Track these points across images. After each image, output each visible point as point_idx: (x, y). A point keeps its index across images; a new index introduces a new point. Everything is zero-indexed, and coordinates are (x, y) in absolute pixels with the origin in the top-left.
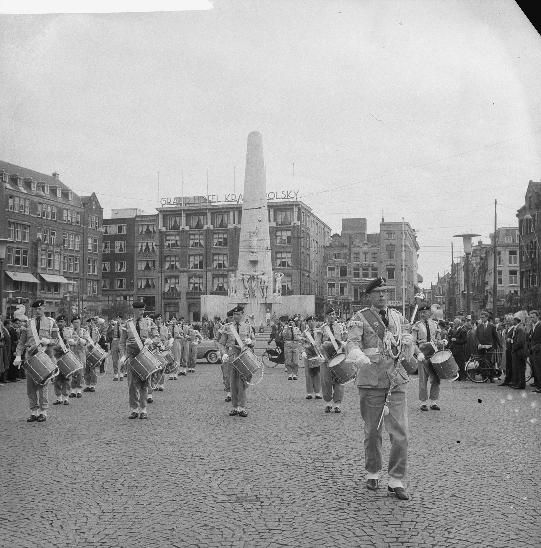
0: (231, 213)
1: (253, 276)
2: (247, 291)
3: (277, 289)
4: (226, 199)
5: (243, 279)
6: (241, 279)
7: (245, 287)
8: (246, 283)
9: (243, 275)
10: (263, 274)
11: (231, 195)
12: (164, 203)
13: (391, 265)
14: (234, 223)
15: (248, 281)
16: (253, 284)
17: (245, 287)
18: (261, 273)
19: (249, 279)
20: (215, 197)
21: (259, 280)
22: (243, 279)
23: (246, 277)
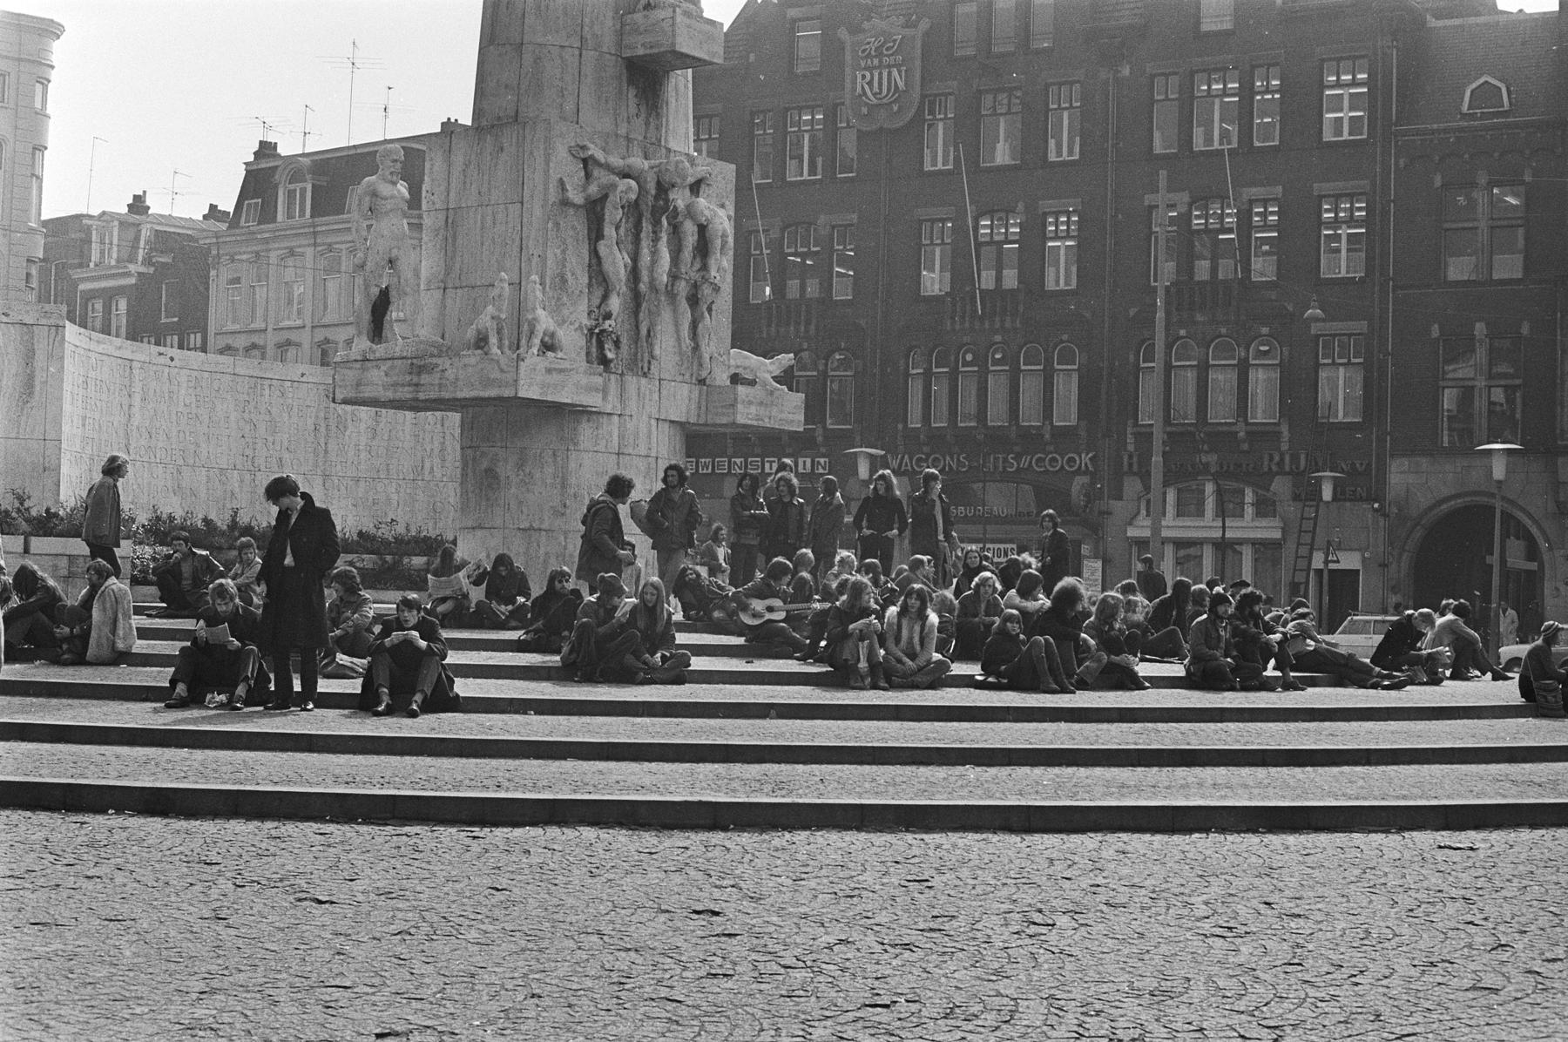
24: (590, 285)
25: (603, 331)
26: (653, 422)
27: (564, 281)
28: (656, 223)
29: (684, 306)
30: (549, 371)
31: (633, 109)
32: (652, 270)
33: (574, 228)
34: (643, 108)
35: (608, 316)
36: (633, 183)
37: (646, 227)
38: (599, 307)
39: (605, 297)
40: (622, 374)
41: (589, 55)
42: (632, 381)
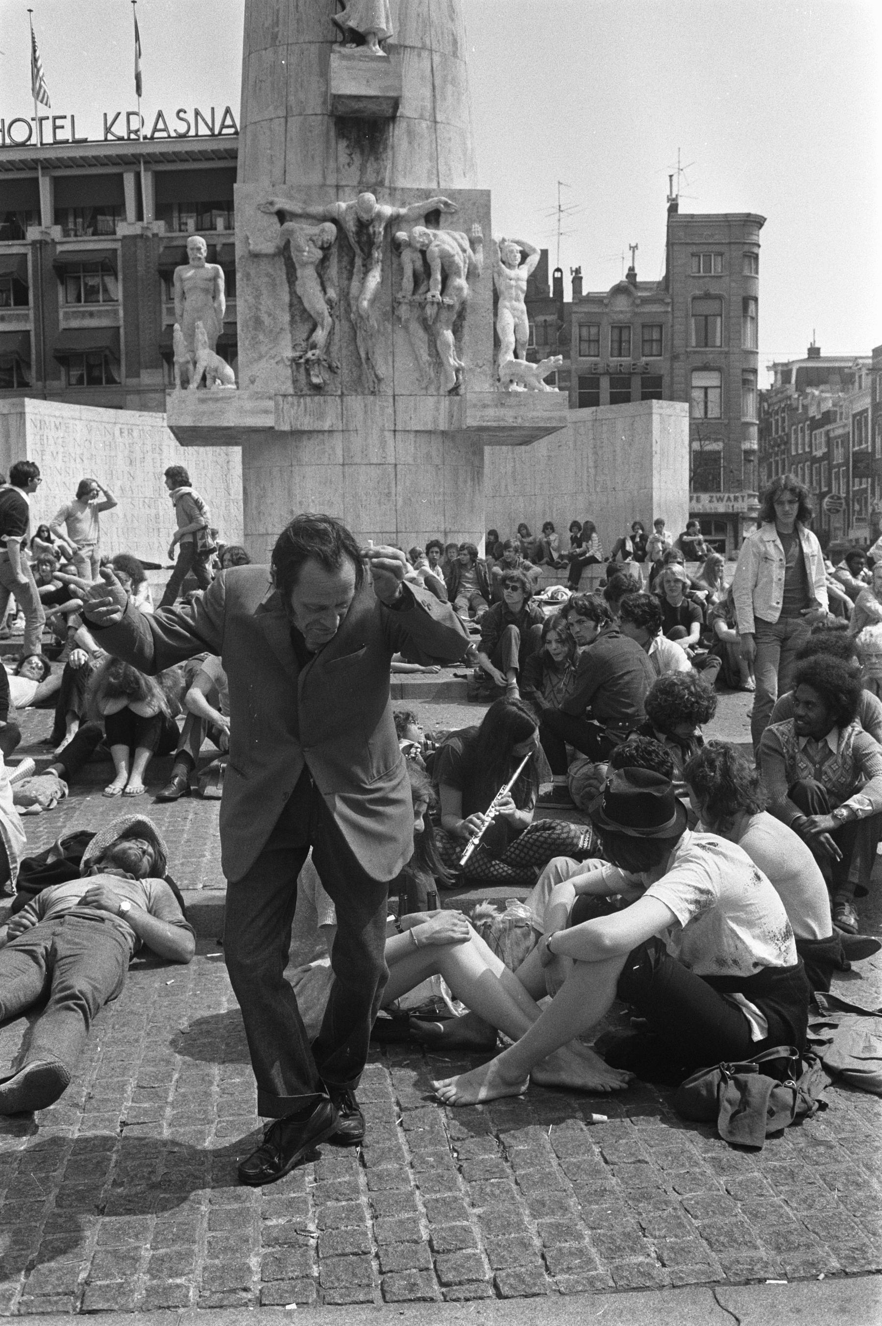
1: (363, 225)
3: (509, 339)
5: (285, 252)
6: (268, 248)
7: (300, 313)
8: (308, 279)
9: (282, 216)
10: (433, 218)
11: (123, 118)
14: (140, 217)
15: (322, 266)
17: (300, 313)
18: (421, 205)
19: (325, 249)
20: (67, 123)
21: (409, 261)
22: (285, 252)
24: (293, 322)
25: (307, 361)
26: (389, 435)
27: (258, 322)
28: (368, 256)
29: (416, 328)
30: (203, 401)
31: (343, 159)
32: (357, 299)
33: (268, 275)
34: (357, 159)
35: (314, 346)
36: (330, 227)
37: (358, 261)
38: (308, 339)
39: (313, 330)
40: (342, 395)
41: (295, 123)
42: (355, 403)
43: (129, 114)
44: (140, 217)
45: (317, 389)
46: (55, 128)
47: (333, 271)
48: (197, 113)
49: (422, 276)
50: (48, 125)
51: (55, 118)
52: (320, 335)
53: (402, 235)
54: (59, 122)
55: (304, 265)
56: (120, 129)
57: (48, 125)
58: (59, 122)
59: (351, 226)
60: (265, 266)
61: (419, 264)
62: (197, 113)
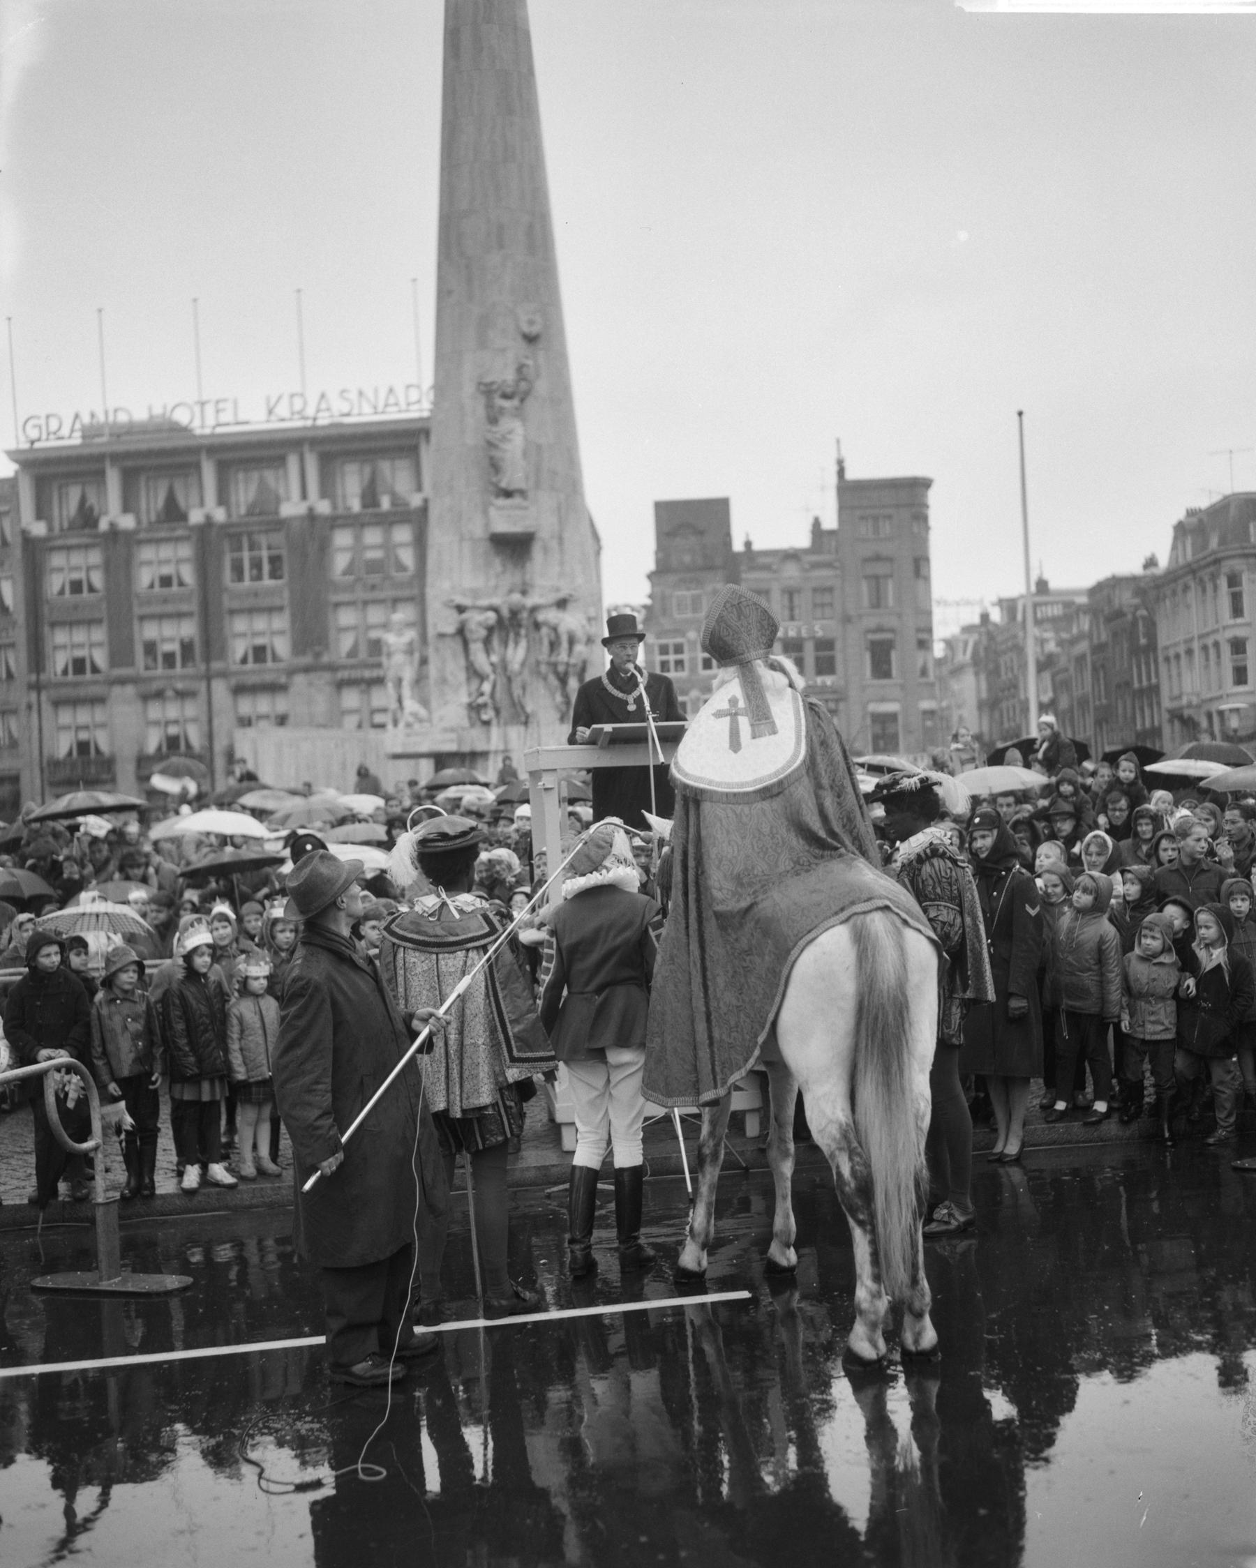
0: (293, 462)
2: (487, 687)
4: (270, 412)
6: (451, 629)
8: (477, 649)
9: (461, 609)
10: (562, 604)
11: (285, 402)
12: (34, 434)
13: (880, 629)
14: (304, 496)
15: (487, 642)
16: (517, 654)
17: (473, 673)
19: (490, 630)
20: (229, 406)
22: (461, 632)
23: (478, 621)
24: (468, 679)
35: (482, 694)
43: (292, 396)
44: (304, 496)
45: (487, 723)
46: (218, 411)
47: (496, 642)
48: (361, 393)
49: (554, 646)
50: (210, 410)
51: (218, 402)
52: (487, 687)
53: (541, 617)
54: (221, 406)
55: (475, 641)
56: (283, 410)
57: (210, 410)
58: (221, 406)
59: (505, 613)
60: (448, 640)
61: (553, 636)
62: (361, 393)
